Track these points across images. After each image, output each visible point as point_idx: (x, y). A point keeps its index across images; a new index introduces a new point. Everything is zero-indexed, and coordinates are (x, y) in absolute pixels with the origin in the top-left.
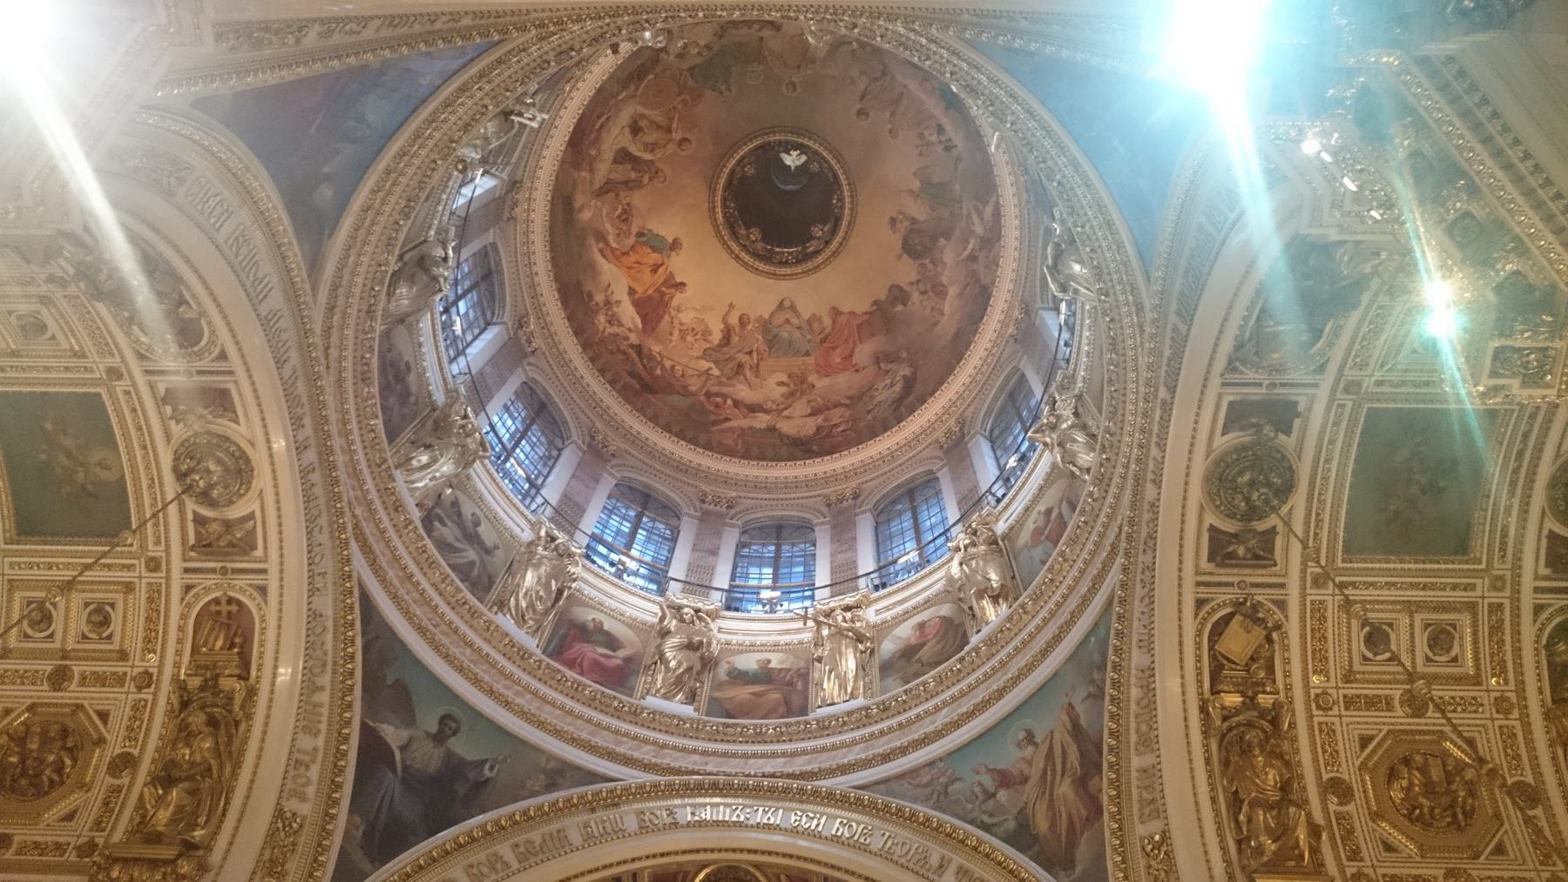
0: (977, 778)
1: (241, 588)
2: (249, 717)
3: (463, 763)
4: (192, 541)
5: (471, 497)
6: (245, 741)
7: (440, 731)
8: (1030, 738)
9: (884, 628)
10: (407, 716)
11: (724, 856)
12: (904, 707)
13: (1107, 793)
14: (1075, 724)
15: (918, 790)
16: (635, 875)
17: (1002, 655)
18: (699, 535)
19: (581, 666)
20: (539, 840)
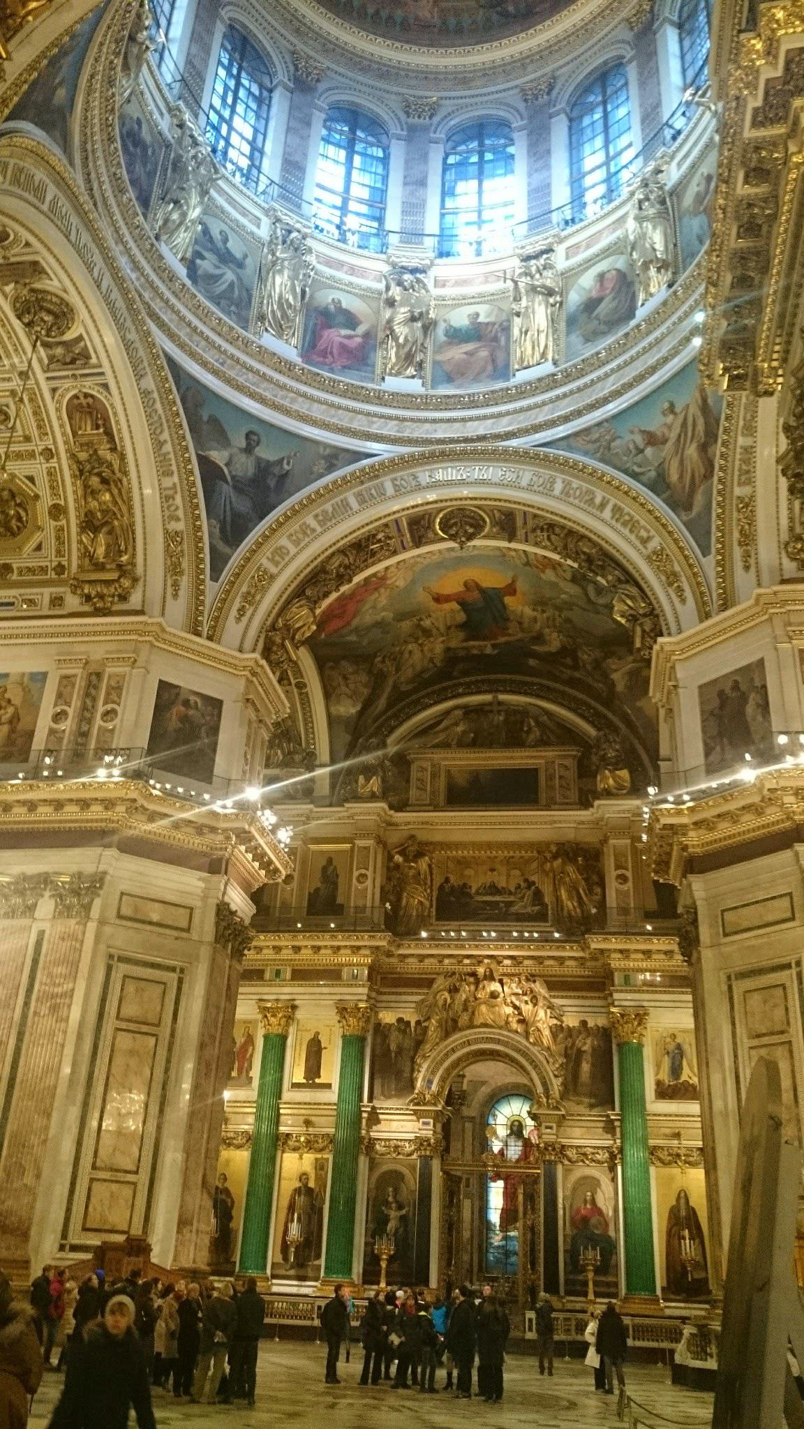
0: (632, 437)
1: (89, 386)
2: (126, 473)
3: (269, 464)
4: (46, 361)
5: (215, 216)
6: (130, 491)
7: (248, 444)
8: (672, 409)
9: (569, 276)
10: (224, 441)
11: (454, 503)
12: (582, 373)
13: (718, 462)
14: (704, 400)
15: (591, 447)
16: (396, 521)
17: (657, 334)
18: (408, 164)
19: (331, 353)
20: (330, 510)
